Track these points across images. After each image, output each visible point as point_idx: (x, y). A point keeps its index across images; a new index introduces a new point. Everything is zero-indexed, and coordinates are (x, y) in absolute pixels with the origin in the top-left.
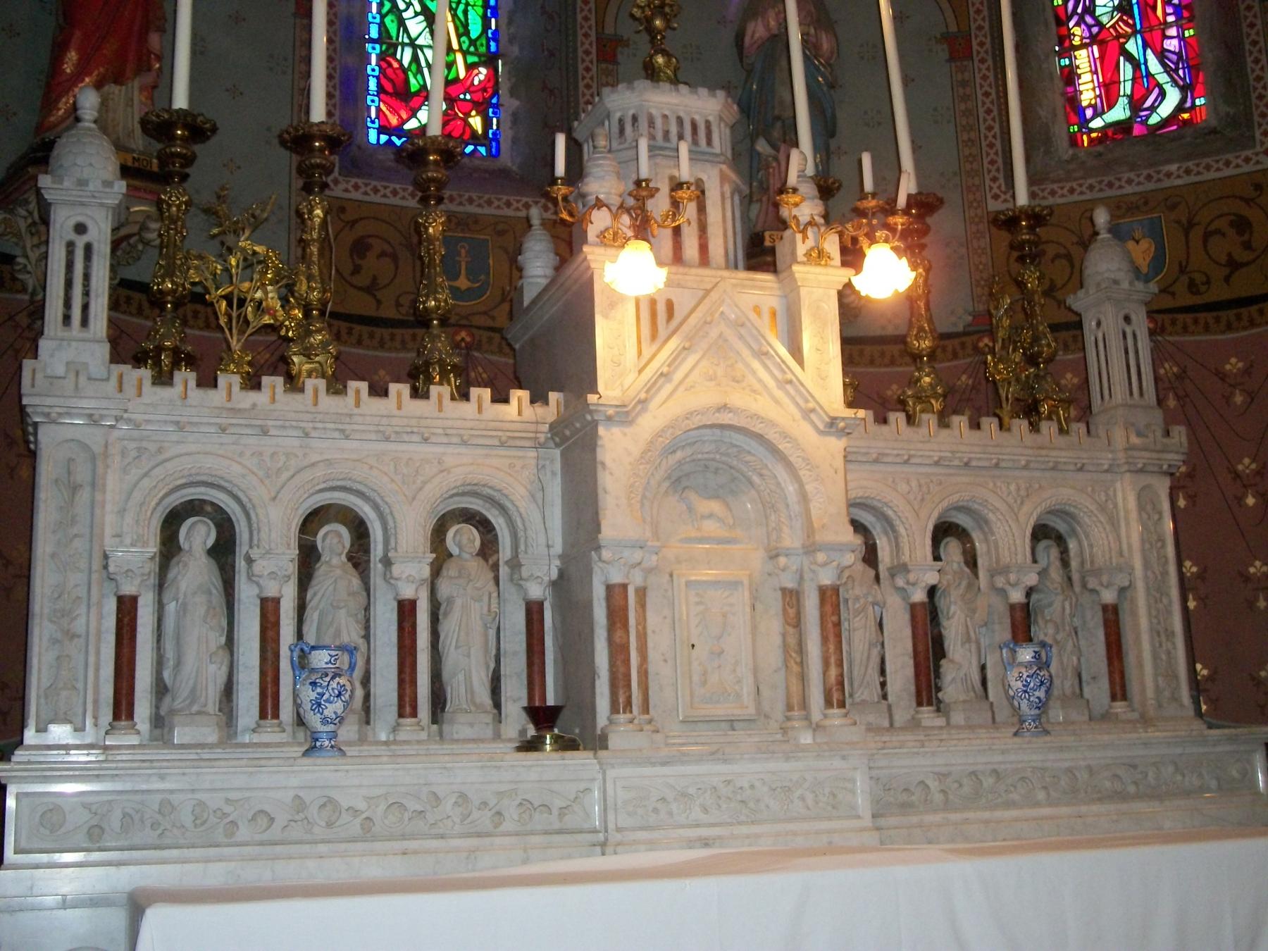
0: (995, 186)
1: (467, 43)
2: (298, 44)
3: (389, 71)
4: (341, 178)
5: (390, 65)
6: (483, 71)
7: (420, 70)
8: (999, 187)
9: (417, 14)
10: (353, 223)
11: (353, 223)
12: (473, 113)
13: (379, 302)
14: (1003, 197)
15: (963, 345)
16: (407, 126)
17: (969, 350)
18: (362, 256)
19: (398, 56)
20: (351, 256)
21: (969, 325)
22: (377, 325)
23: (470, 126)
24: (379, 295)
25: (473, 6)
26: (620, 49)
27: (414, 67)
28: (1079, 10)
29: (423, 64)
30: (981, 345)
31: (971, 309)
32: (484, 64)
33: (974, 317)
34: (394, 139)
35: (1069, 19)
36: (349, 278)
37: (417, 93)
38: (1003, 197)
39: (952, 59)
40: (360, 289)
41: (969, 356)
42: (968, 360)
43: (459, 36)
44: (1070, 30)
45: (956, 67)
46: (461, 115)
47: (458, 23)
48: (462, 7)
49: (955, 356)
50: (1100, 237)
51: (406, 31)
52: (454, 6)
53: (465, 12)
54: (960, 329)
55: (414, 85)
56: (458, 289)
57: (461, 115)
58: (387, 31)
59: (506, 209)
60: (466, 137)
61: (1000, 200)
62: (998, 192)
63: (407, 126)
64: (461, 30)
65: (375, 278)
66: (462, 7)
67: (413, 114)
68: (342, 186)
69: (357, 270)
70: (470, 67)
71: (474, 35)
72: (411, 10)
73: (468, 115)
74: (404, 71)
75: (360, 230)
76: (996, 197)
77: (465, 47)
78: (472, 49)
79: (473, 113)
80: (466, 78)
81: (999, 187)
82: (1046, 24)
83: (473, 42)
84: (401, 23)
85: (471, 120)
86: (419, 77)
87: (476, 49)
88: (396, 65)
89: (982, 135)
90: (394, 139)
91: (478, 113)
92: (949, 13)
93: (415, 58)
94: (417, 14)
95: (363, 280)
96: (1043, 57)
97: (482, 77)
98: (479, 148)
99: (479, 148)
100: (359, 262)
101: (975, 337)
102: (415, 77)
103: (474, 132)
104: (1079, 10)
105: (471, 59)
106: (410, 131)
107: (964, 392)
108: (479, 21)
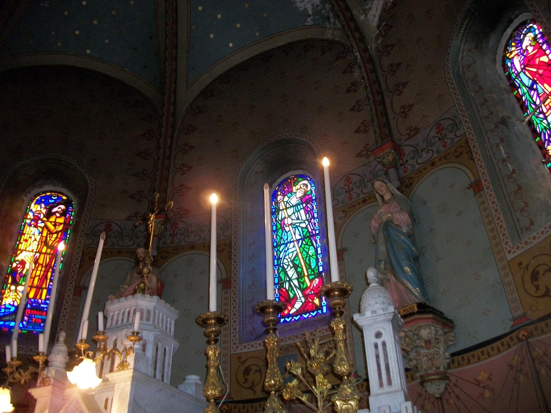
0: (507, 246)
1: (310, 271)
2: (223, 299)
3: (283, 294)
4: (239, 345)
5: (282, 291)
6: (317, 280)
7: (293, 289)
8: (509, 246)
9: (291, 268)
10: (244, 362)
11: (244, 362)
12: (315, 298)
13: (255, 392)
14: (513, 250)
15: (512, 339)
16: (291, 312)
17: (515, 341)
18: (248, 374)
19: (285, 287)
20: (244, 374)
21: (513, 326)
22: (260, 401)
23: (314, 303)
24: (255, 389)
25: (312, 256)
26: (344, 253)
27: (290, 289)
28: (547, 138)
29: (293, 286)
30: (520, 336)
31: (511, 317)
32: (317, 277)
33: (514, 321)
34: (286, 319)
35: (544, 144)
36: (243, 385)
37: (293, 298)
38: (513, 250)
39: (475, 193)
40: (247, 388)
41: (516, 344)
42: (516, 346)
43: (307, 270)
44: (546, 149)
45: (478, 196)
46: (311, 301)
47: (306, 265)
48: (308, 258)
49: (509, 346)
50: (371, 285)
51: (288, 276)
52: (305, 259)
53: (309, 260)
54: (508, 330)
55: (291, 295)
56: (285, 378)
57: (311, 301)
58: (281, 278)
59: (289, 341)
60: (314, 309)
61: (512, 252)
62: (510, 249)
63: (291, 312)
64: (308, 267)
65: (253, 382)
66: (308, 258)
67: (293, 307)
68: (239, 348)
69: (246, 380)
70: (311, 281)
71: (313, 267)
72: (289, 267)
73: (313, 299)
74: (287, 291)
75: (247, 364)
76: (509, 252)
77: (310, 273)
78: (312, 273)
79: (315, 298)
80: (310, 286)
81: (509, 246)
82: (534, 152)
83: (313, 270)
84: (286, 274)
85: (315, 301)
86: (293, 292)
87: (314, 272)
88: (284, 290)
89: (496, 223)
90: (286, 319)
91: (317, 298)
92: (470, 175)
93: (290, 285)
94: (291, 268)
95: (248, 385)
96: (535, 169)
97: (317, 283)
98: (319, 311)
99: (319, 311)
100: (246, 377)
101: (516, 332)
102: (291, 292)
103: (316, 305)
104: (547, 138)
105: (311, 277)
106: (293, 314)
107: (517, 366)
108: (315, 261)
